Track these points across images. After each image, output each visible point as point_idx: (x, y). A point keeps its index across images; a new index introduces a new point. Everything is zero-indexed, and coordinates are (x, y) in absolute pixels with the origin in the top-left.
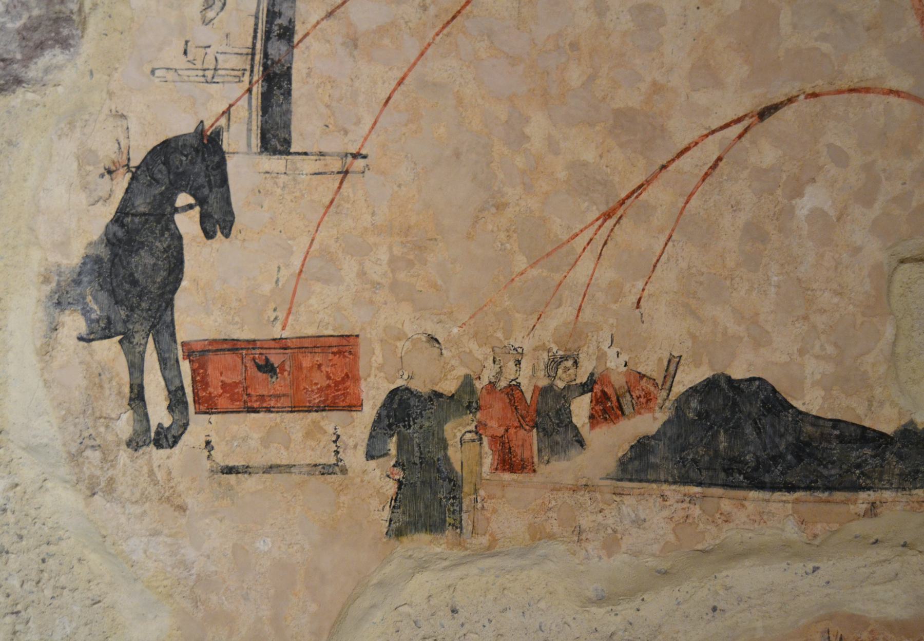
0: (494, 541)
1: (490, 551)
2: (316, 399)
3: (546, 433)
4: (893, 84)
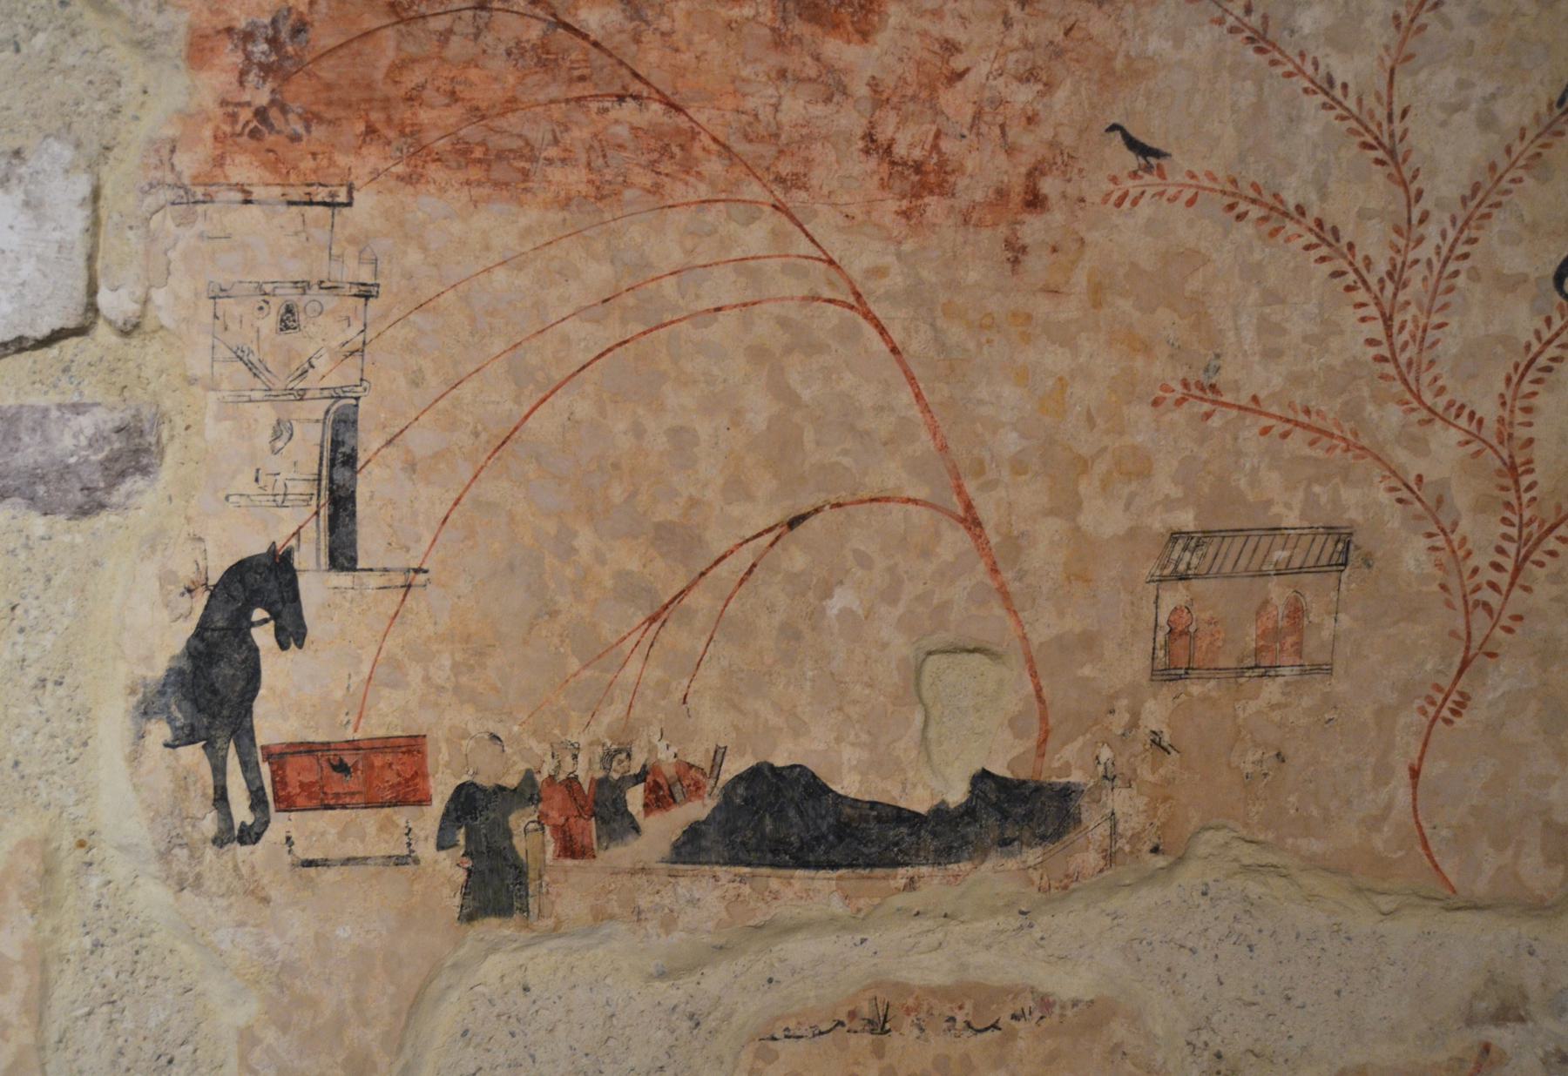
0: (558, 924)
1: (555, 932)
2: (388, 795)
3: (603, 821)
4: (911, 493)
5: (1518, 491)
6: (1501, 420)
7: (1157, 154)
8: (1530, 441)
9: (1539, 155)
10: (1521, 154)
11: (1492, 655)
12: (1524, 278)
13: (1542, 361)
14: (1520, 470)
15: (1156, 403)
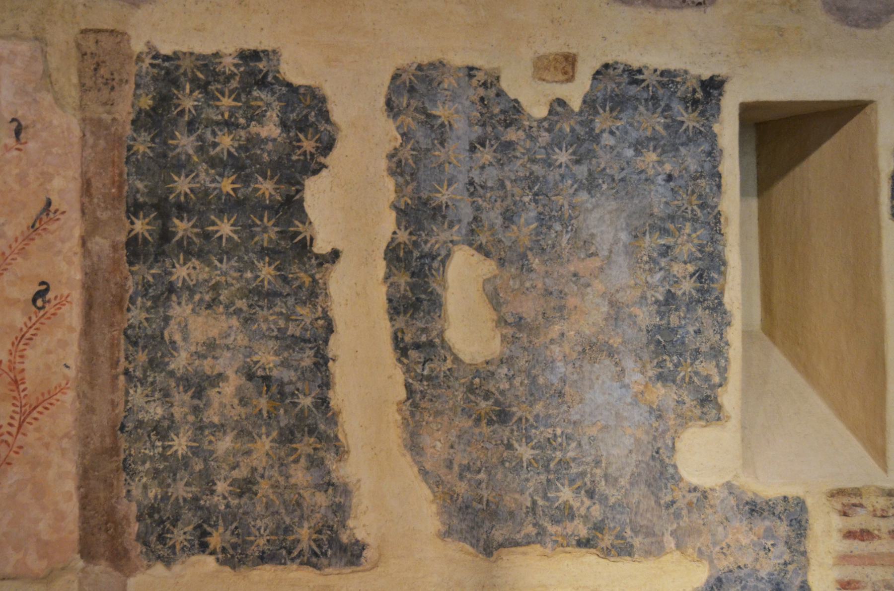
5: (19, 392)
6: (10, 361)
8: (23, 370)
9: (24, 248)
10: (17, 247)
11: (9, 464)
12: (19, 301)
13: (28, 335)
14: (19, 382)
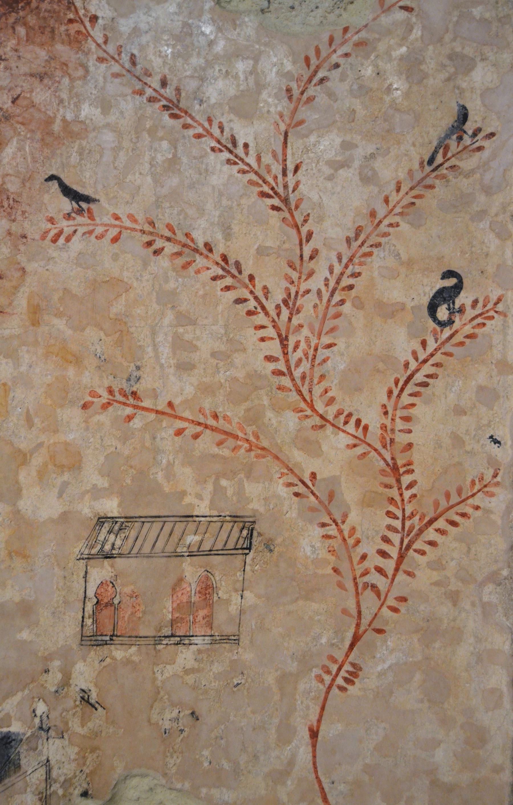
5: (400, 488)
6: (384, 427)
7: (87, 199)
8: (410, 446)
9: (413, 204)
10: (398, 203)
11: (380, 631)
12: (403, 307)
13: (419, 377)
14: (402, 470)
15: (85, 406)
